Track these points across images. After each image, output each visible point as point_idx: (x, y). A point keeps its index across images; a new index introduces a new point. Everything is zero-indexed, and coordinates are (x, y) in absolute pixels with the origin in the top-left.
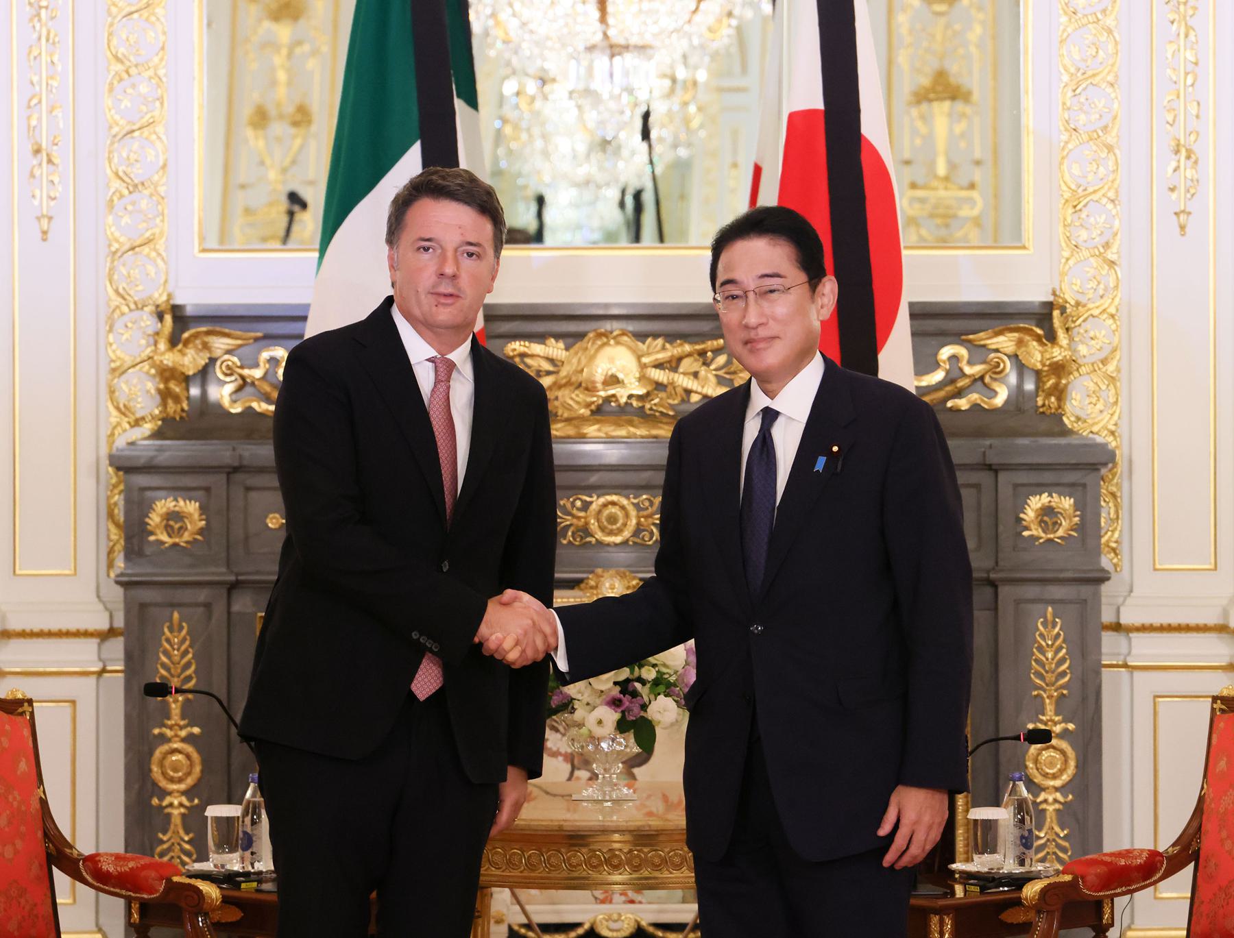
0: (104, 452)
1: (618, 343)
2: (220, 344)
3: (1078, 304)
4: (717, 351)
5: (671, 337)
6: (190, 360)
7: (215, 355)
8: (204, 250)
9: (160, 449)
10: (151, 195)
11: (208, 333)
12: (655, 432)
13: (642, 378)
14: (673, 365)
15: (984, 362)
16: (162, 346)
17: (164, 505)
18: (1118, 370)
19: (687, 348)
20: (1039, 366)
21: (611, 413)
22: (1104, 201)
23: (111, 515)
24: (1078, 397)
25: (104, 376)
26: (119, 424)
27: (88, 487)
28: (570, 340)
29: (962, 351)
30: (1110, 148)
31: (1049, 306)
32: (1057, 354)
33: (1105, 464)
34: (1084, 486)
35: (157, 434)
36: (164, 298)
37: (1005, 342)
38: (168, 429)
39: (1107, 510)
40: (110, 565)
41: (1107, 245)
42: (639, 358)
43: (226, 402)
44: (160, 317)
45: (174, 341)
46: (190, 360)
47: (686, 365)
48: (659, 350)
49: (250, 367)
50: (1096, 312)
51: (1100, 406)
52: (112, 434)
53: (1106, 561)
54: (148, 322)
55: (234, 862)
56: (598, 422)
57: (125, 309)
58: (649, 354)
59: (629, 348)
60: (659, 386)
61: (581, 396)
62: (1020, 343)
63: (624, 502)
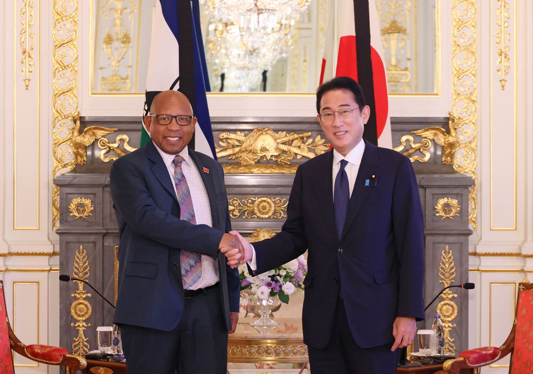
0: (51, 178)
1: (267, 134)
2: (100, 133)
3: (459, 118)
4: (308, 137)
5: (289, 131)
6: (87, 140)
8: (93, 94)
9: (75, 177)
10: (71, 71)
11: (95, 128)
12: (282, 171)
13: (277, 149)
14: (290, 143)
15: (420, 143)
16: (76, 134)
17: (76, 201)
18: (476, 146)
19: (296, 136)
20: (443, 144)
22: (470, 75)
23: (54, 204)
24: (459, 157)
25: (51, 146)
26: (57, 166)
28: (247, 132)
29: (411, 138)
30: (473, 53)
31: (448, 119)
32: (451, 139)
33: (470, 186)
34: (462, 195)
35: (74, 171)
36: (76, 114)
37: (429, 134)
39: (471, 205)
40: (54, 225)
41: (471, 94)
42: (275, 140)
43: (102, 157)
44: (75, 122)
45: (81, 132)
46: (87, 140)
47: (295, 143)
48: (283, 137)
49: (112, 143)
50: (467, 122)
51: (468, 161)
52: (55, 171)
53: (471, 226)
54: (71, 124)
56: (258, 167)
57: (60, 118)
59: (271, 135)
60: (284, 152)
61: (251, 156)
62: (435, 134)
63: (269, 200)
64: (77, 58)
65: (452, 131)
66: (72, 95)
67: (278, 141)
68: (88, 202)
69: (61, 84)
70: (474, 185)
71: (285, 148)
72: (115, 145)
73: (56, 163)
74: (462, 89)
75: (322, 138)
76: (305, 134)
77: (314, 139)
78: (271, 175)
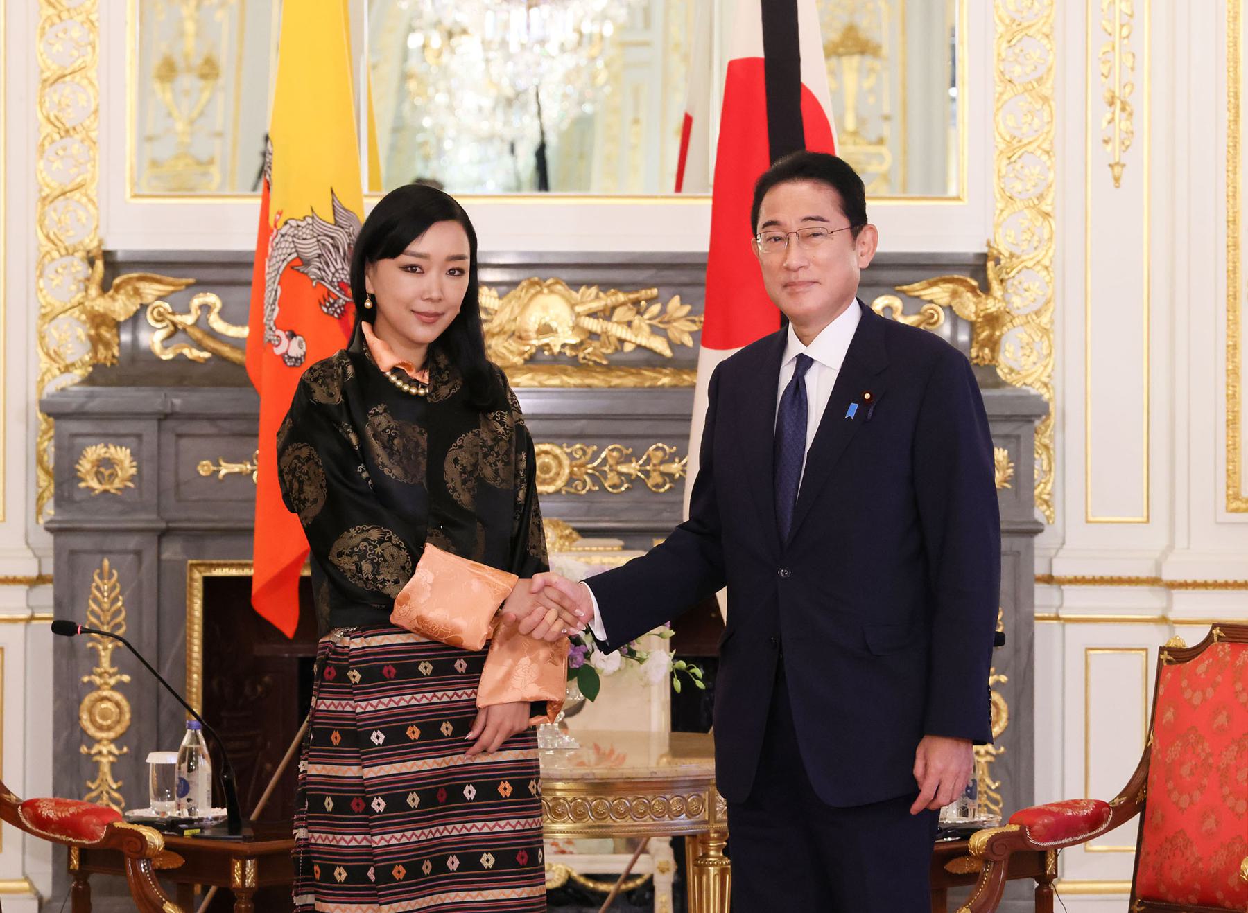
0: (34, 398)
1: (552, 292)
2: (150, 291)
3: (1012, 256)
4: (651, 301)
5: (604, 286)
6: (120, 306)
7: (145, 302)
8: (135, 196)
9: (91, 396)
10: (82, 141)
11: (141, 279)
12: (588, 381)
13: (576, 327)
14: (607, 314)
15: (918, 313)
16: (94, 291)
17: (95, 452)
18: (1052, 322)
19: (621, 297)
20: (973, 318)
21: (545, 362)
22: (1039, 152)
23: (40, 462)
24: (1012, 349)
25: (34, 320)
26: (48, 370)
27: (18, 433)
28: (504, 289)
29: (896, 303)
30: (1045, 100)
31: (984, 257)
32: (992, 306)
33: (1039, 416)
34: (1018, 437)
35: (89, 380)
36: (95, 243)
37: (940, 293)
38: (98, 375)
39: (1041, 462)
40: (39, 512)
41: (1041, 197)
42: (572, 307)
43: (157, 348)
44: (91, 263)
45: (105, 287)
46: (120, 306)
47: (620, 314)
48: (592, 299)
49: (182, 313)
50: (1030, 264)
51: (1033, 358)
52: (42, 380)
53: (1040, 513)
54: (81, 268)
55: (170, 809)
56: (530, 370)
57: (55, 254)
58: (582, 303)
59: (563, 296)
60: (593, 335)
61: (514, 345)
62: (954, 294)
63: (558, 451)
64: (96, 112)
65: (995, 286)
66: (84, 200)
67: (579, 309)
68: (122, 455)
69: (52, 174)
70: (1048, 414)
71: (594, 325)
72: (189, 320)
73: (44, 363)
74: (1018, 186)
75: (683, 302)
76: (644, 293)
77: (665, 305)
78: (561, 392)
